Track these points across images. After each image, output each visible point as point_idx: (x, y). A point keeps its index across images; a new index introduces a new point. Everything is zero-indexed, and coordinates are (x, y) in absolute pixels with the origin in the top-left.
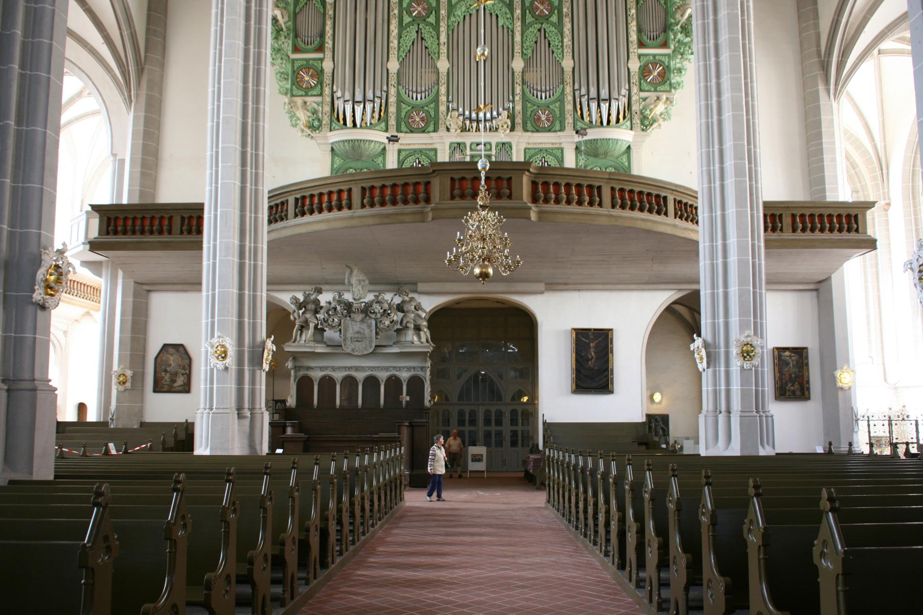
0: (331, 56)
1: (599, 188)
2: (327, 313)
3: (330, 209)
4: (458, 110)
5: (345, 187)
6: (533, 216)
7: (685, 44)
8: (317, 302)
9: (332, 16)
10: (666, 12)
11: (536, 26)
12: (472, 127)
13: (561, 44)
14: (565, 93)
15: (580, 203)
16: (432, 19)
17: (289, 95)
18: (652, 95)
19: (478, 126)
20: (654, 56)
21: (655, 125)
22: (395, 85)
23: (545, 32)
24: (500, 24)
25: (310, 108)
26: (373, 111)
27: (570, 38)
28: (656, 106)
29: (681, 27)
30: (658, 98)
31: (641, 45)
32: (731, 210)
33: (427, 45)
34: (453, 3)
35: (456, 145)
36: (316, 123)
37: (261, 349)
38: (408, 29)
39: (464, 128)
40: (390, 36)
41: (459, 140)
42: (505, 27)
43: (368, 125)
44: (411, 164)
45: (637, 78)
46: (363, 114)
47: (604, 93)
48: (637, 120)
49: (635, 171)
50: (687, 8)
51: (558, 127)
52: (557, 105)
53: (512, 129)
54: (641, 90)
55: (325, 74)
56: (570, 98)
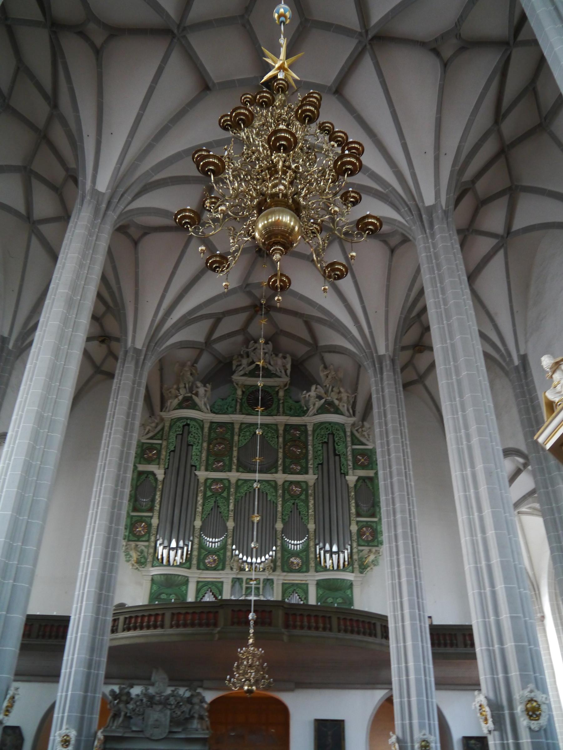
1: (330, 617)
2: (135, 703)
3: (148, 627)
5: (160, 612)
6: (285, 638)
8: (128, 694)
11: (291, 501)
13: (307, 514)
15: (317, 628)
16: (225, 494)
17: (126, 540)
18: (366, 549)
20: (367, 522)
21: (369, 569)
24: (269, 499)
26: (182, 555)
28: (369, 556)
30: (370, 551)
31: (358, 515)
32: (409, 643)
35: (236, 580)
36: (143, 560)
37: (93, 739)
38: (209, 500)
41: (239, 576)
47: (335, 549)
48: (356, 565)
51: (304, 569)
52: (305, 553)
54: (359, 545)
56: (313, 549)
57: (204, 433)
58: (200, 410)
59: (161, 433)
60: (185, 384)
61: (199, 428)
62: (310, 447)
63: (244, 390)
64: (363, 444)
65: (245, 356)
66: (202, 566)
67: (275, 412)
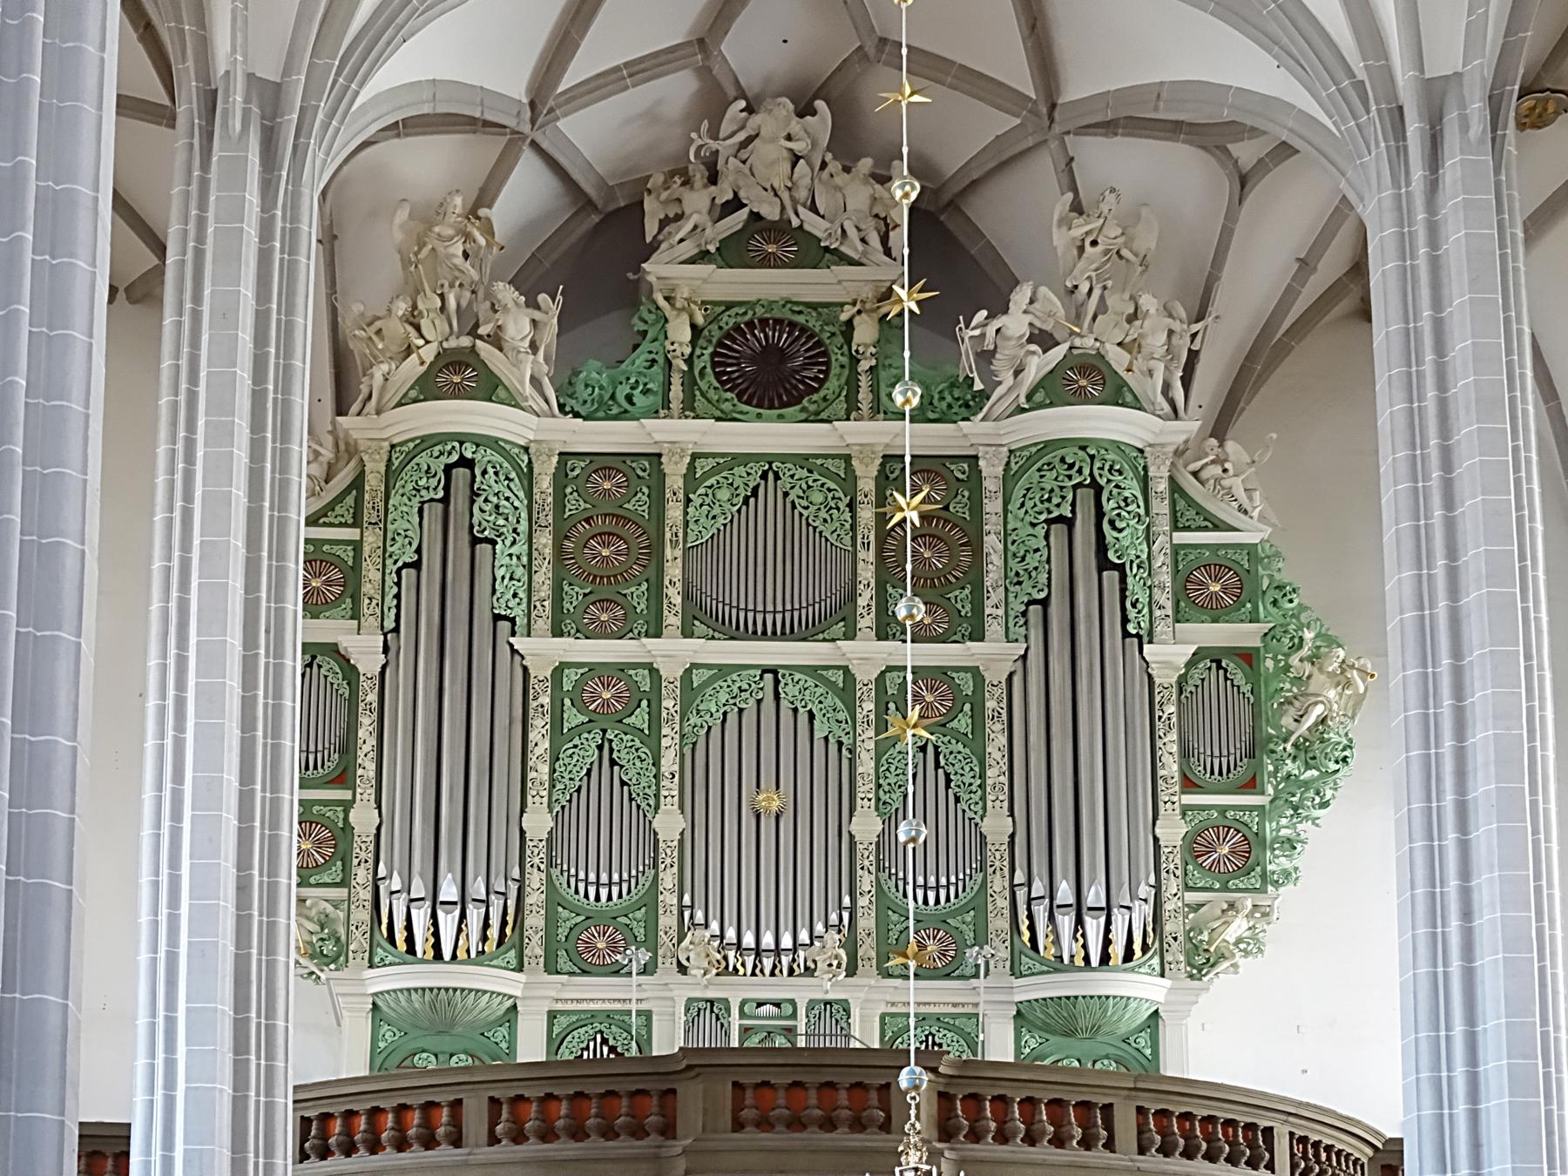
0: (373, 797)
4: (707, 926)
7: (1306, 785)
9: (375, 705)
10: (1256, 716)
12: (743, 965)
13: (979, 782)
14: (990, 891)
16: (640, 719)
19: (760, 962)
21: (1225, 965)
22: (543, 867)
23: (937, 754)
24: (819, 734)
25: (313, 913)
27: (1005, 768)
28: (1227, 923)
29: (1295, 745)
31: (1189, 785)
33: (625, 778)
34: (695, 685)
35: (702, 1005)
38: (576, 741)
39: (724, 964)
40: (530, 755)
41: (711, 994)
42: (832, 740)
43: (473, 955)
44: (584, 1045)
45: (1178, 861)
46: (460, 930)
48: (1176, 954)
49: (1170, 1069)
50: (1316, 703)
52: (969, 918)
53: (852, 971)
54: (1188, 888)
55: (356, 838)
57: (537, 497)
58: (513, 402)
59: (350, 500)
60: (442, 296)
61: (513, 475)
62: (992, 543)
63: (700, 320)
64: (1218, 526)
65: (699, 174)
66: (563, 962)
67: (840, 406)
